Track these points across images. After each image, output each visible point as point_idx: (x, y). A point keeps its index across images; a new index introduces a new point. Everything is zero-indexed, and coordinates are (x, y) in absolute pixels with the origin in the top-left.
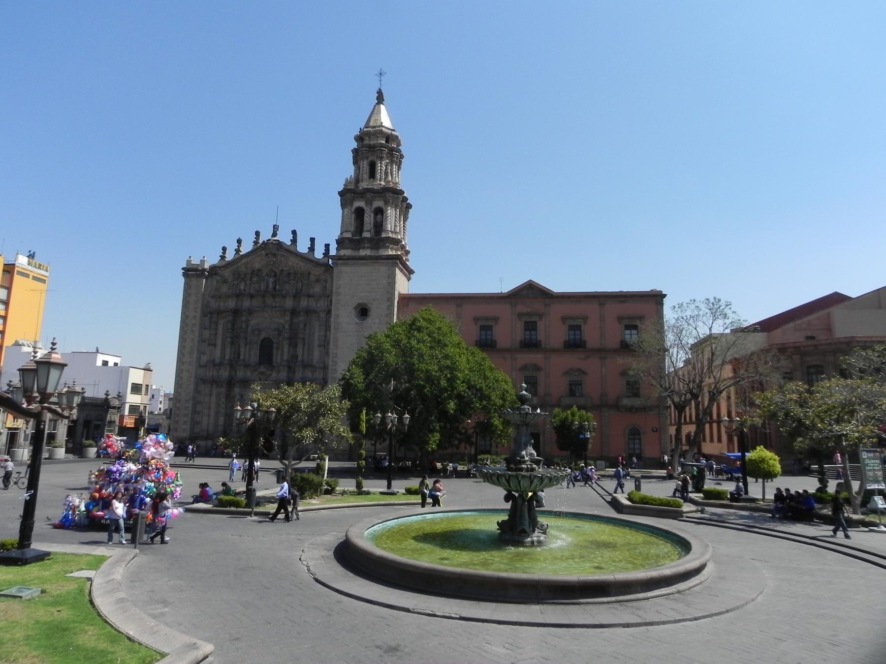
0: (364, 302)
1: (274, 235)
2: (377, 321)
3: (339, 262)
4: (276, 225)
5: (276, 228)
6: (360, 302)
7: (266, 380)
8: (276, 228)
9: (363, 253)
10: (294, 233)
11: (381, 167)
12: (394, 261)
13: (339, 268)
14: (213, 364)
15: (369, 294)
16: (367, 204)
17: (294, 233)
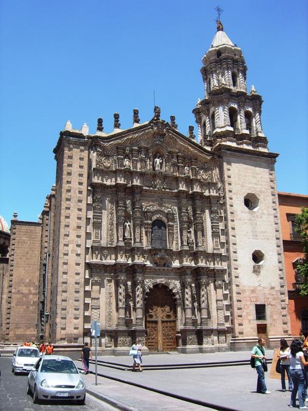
0: (253, 193)
1: (158, 116)
2: (265, 211)
3: (228, 152)
4: (157, 108)
5: (157, 111)
6: (250, 192)
7: (164, 265)
8: (157, 111)
9: (245, 147)
10: (173, 118)
11: (240, 78)
12: (273, 159)
13: (227, 158)
14: (96, 249)
15: (256, 186)
16: (239, 106)
17: (173, 118)
